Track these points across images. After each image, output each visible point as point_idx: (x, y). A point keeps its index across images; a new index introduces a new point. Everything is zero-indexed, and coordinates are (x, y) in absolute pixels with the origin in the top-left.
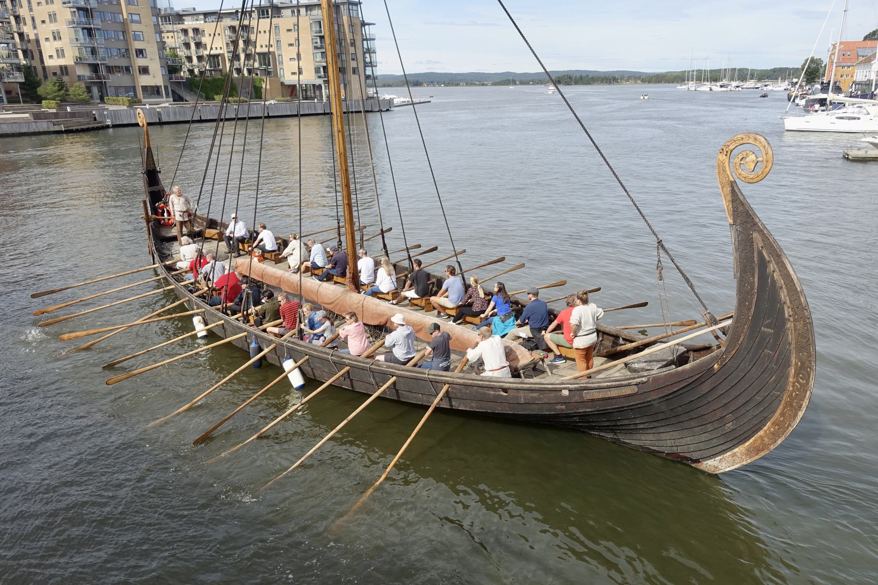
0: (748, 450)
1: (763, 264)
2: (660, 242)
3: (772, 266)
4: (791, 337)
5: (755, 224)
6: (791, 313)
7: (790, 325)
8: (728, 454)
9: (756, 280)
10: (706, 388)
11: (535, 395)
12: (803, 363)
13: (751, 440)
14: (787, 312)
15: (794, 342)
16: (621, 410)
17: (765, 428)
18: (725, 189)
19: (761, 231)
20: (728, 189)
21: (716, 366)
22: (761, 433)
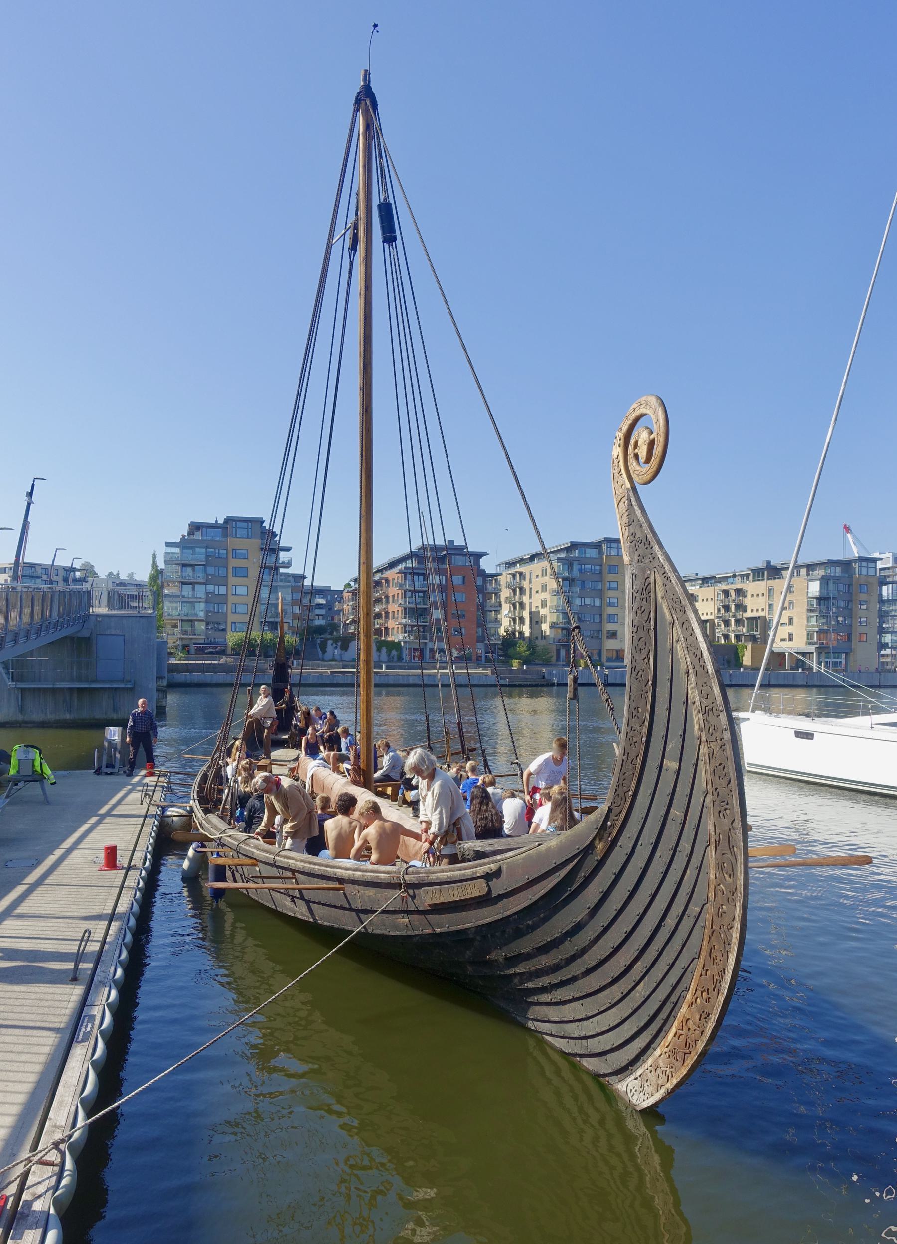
0: (673, 1053)
6: (702, 724)
7: (704, 750)
8: (650, 1061)
9: (652, 660)
10: (592, 893)
13: (674, 1030)
14: (696, 720)
15: (710, 786)
17: (689, 996)
18: (621, 504)
22: (683, 1010)
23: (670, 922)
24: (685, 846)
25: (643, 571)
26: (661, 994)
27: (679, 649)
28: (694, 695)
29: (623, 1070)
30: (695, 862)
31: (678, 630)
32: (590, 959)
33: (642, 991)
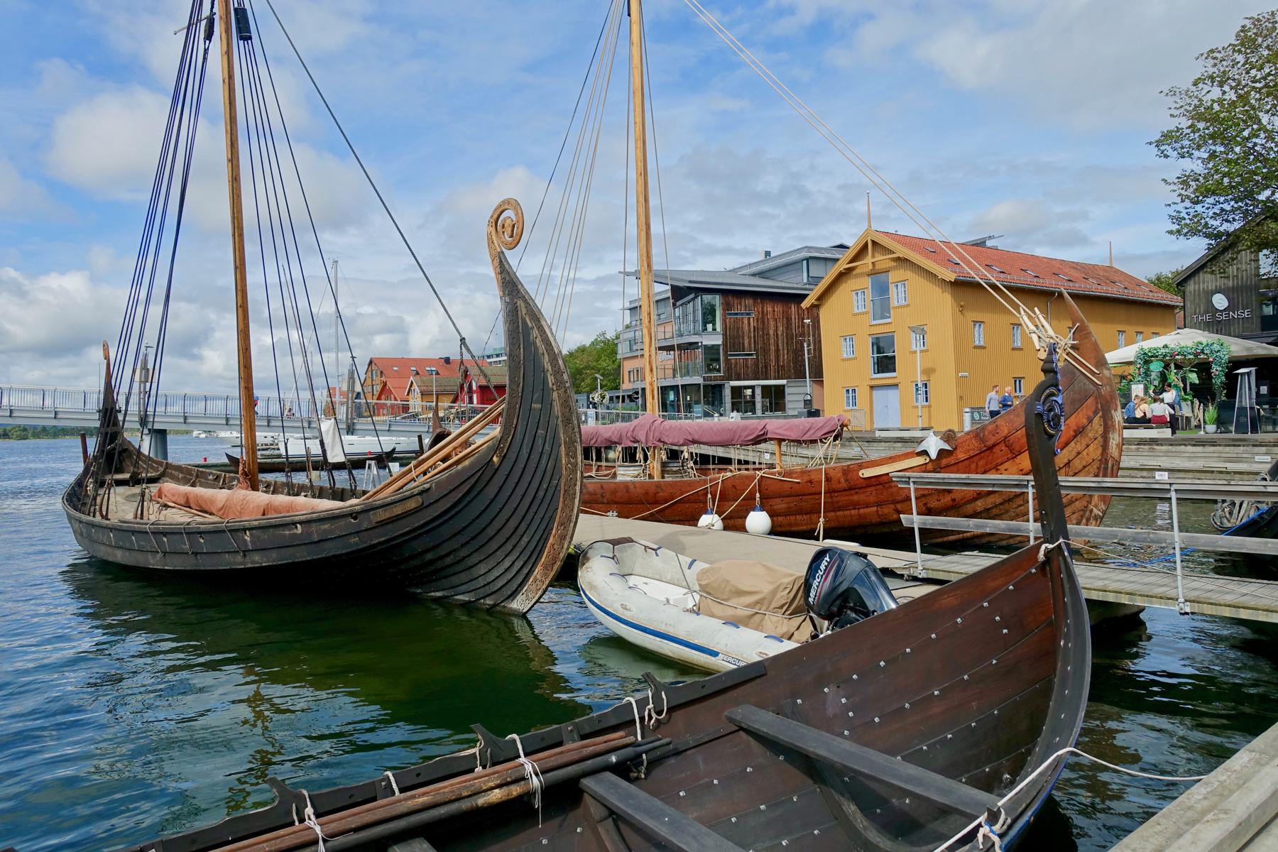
0: (545, 568)
1: (527, 330)
2: (463, 340)
3: (535, 332)
4: (557, 408)
5: (519, 291)
7: (555, 395)
10: (491, 490)
11: (326, 526)
12: (570, 438)
14: (551, 379)
16: (416, 534)
19: (525, 301)
20: (497, 261)
21: (495, 459)
22: (551, 540)
23: (541, 494)
24: (547, 447)
25: (512, 299)
26: (537, 537)
27: (538, 342)
28: (548, 366)
29: (513, 595)
30: (553, 457)
31: (535, 332)
32: (490, 531)
33: (525, 539)
